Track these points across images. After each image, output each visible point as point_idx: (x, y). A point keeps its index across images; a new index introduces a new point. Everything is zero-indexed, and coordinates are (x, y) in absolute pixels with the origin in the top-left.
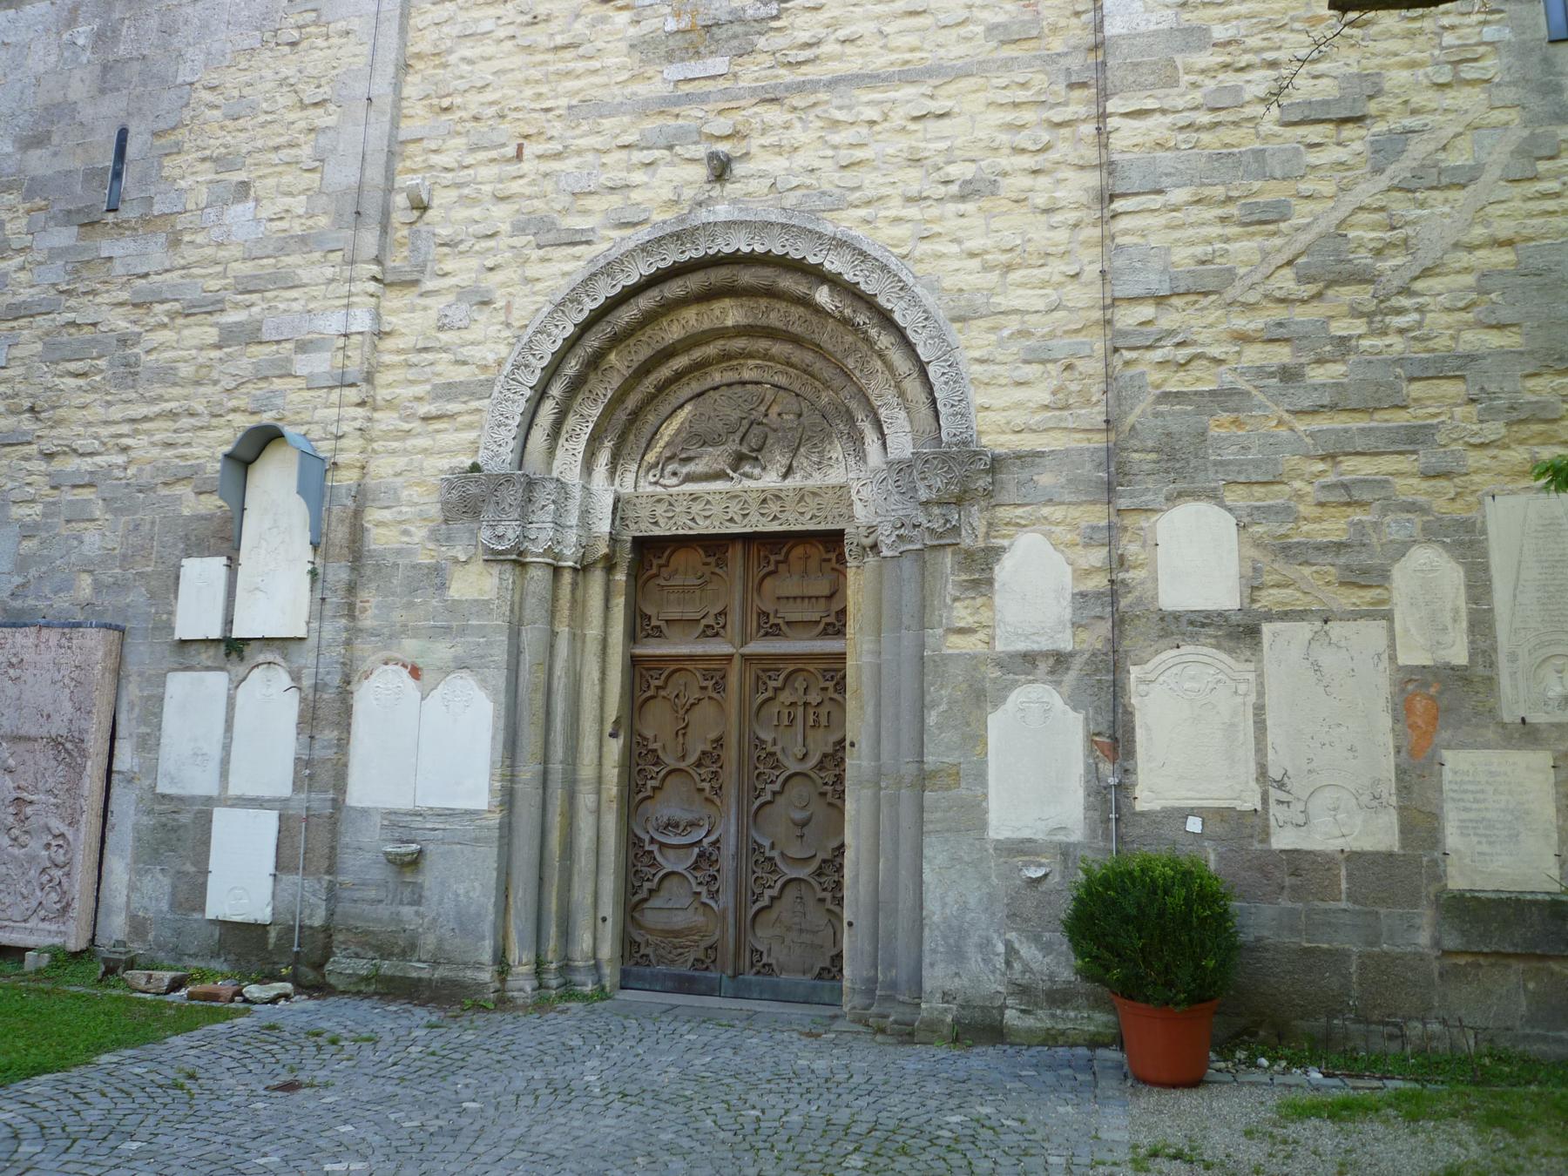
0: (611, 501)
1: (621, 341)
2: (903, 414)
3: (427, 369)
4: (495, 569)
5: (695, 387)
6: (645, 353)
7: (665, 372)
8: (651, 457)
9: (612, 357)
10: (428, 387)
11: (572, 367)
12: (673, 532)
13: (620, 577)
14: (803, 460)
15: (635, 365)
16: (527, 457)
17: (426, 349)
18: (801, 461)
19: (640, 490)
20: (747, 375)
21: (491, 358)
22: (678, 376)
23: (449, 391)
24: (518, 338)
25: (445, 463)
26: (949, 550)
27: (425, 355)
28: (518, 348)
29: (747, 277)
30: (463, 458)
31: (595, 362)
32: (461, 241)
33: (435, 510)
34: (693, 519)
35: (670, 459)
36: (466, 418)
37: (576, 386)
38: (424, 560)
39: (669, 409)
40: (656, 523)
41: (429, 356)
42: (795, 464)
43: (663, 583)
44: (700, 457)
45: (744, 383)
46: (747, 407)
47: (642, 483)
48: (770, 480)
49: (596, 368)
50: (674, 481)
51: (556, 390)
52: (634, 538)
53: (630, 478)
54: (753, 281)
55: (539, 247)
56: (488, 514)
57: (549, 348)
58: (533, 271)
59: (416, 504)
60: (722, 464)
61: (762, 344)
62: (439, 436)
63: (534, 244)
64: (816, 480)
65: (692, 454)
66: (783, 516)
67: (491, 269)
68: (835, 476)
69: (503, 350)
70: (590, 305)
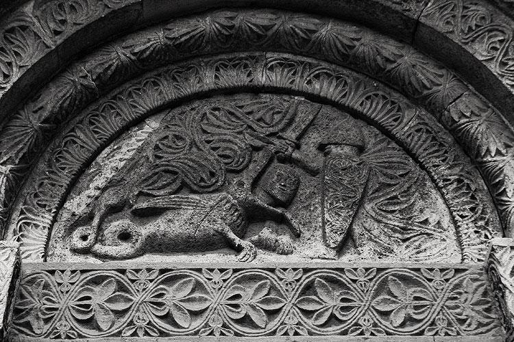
5: (169, 92)
7: (119, 54)
8: (77, 205)
14: (370, 223)
15: (69, 30)
18: (366, 225)
34: (168, 318)
35: (114, 210)
39: (116, 123)
42: (357, 230)
44: (176, 208)
45: (255, 90)
46: (263, 130)
48: (312, 252)
50: (125, 248)
53: (35, 240)
60: (218, 224)
64: (401, 258)
65: (160, 203)
66: (349, 317)
68: (440, 252)
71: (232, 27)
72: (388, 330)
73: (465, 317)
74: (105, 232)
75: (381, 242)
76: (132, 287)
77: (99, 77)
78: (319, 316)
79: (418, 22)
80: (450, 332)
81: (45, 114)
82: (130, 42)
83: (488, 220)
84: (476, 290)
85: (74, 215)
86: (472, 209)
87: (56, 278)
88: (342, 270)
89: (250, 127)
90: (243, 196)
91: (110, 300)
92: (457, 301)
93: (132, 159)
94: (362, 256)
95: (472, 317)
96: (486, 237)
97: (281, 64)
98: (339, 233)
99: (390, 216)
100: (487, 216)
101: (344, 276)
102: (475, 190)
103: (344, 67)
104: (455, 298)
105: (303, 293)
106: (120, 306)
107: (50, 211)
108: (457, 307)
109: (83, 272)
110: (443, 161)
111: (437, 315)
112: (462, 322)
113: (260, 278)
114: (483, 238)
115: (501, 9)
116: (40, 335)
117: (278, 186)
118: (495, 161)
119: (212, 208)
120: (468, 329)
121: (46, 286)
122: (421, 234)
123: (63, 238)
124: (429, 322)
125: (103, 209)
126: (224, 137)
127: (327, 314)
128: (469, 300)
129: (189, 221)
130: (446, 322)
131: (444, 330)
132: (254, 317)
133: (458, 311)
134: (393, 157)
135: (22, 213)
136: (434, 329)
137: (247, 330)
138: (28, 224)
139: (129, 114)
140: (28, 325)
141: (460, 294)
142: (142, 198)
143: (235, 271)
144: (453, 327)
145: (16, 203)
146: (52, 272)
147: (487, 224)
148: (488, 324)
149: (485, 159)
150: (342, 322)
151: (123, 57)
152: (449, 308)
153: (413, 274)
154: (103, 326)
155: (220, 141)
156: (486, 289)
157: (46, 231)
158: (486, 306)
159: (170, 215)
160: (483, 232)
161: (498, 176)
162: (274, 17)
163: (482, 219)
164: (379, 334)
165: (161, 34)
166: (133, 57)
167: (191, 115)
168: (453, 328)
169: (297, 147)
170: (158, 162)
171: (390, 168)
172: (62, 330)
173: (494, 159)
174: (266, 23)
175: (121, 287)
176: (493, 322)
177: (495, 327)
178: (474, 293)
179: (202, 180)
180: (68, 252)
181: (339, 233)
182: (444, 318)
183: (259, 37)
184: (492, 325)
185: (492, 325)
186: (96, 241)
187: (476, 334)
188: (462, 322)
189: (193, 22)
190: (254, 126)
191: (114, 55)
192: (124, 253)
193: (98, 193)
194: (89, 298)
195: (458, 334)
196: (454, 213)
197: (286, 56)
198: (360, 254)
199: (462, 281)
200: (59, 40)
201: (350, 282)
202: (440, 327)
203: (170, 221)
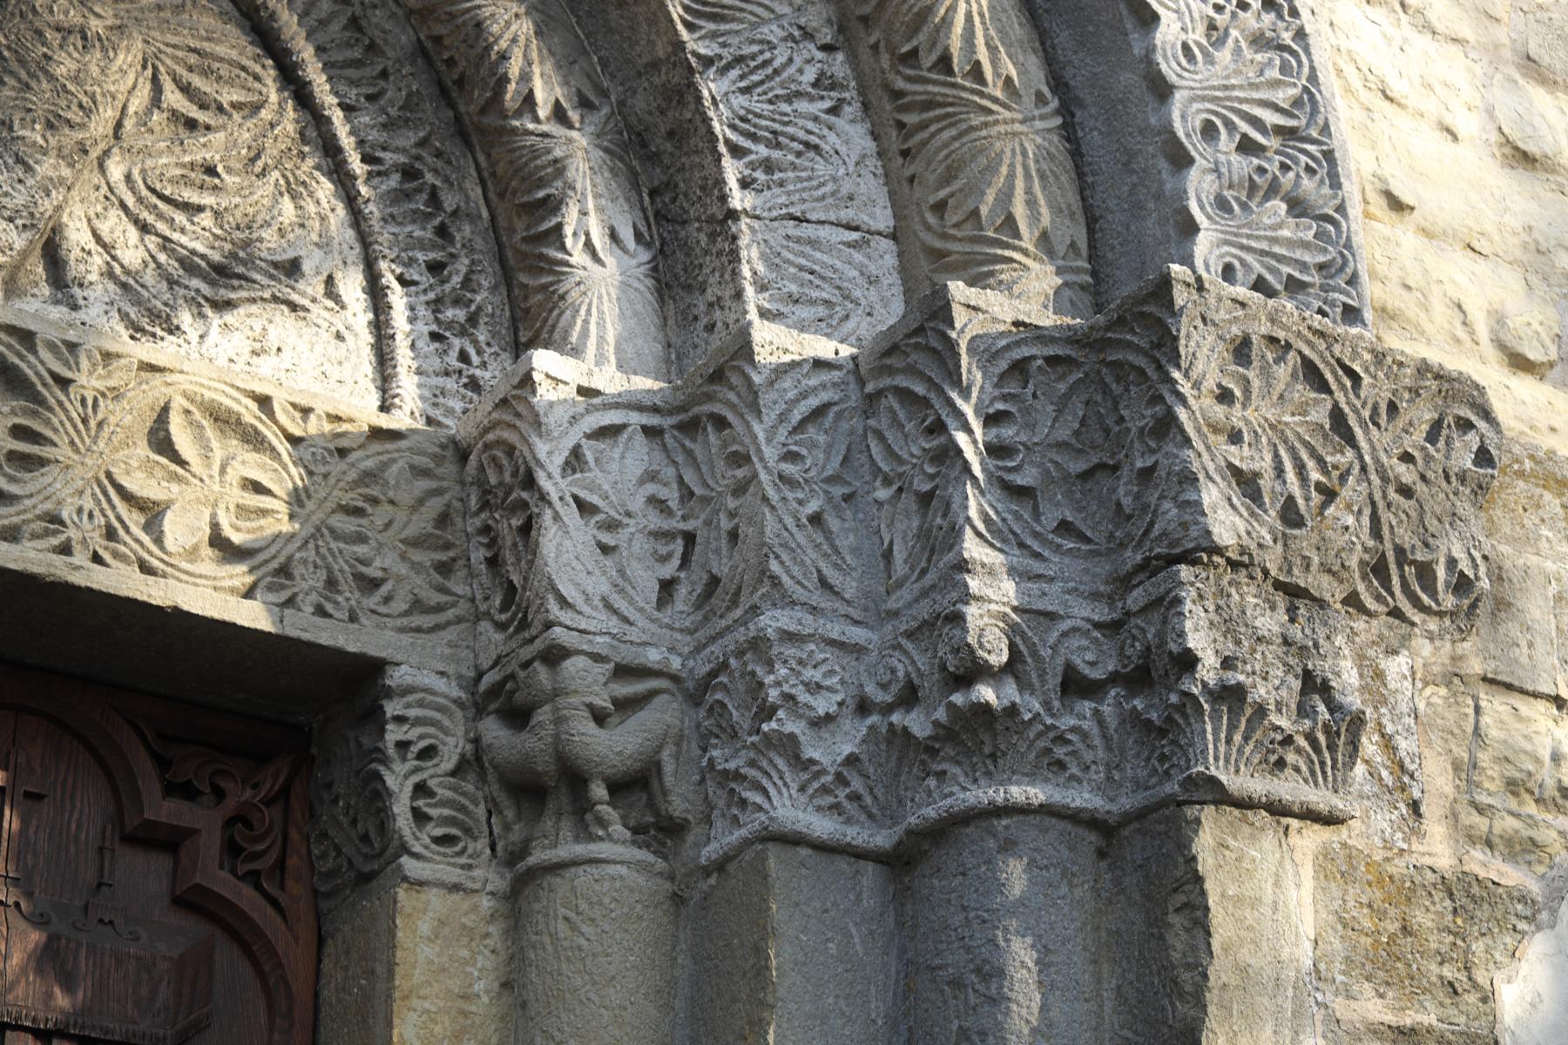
2: (851, 137)
26: (1309, 839)
72: (146, 556)
73: (379, 574)
75: (146, 294)
80: (329, 607)
83: (479, 308)
84: (421, 501)
92: (364, 521)
94: (81, 315)
95: (400, 579)
96: (464, 357)
98: (19, 222)
99: (180, 218)
100: (478, 298)
101: (31, 358)
102: (455, 213)
104: (358, 512)
108: (361, 539)
110: (369, 98)
111: (300, 549)
112: (370, 584)
114: (452, 360)
118: (545, 135)
120: (383, 609)
122: (275, 299)
124: (275, 564)
128: (396, 526)
130: (322, 575)
131: (314, 597)
133: (361, 550)
134: (219, 41)
136: (283, 587)
141: (375, 501)
144: (339, 592)
147: (473, 320)
148: (439, 609)
149: (516, 123)
152: (336, 535)
153: (249, 412)
156: (448, 506)
158: (443, 556)
160: (457, 343)
161: (542, 183)
163: (457, 302)
164: (121, 565)
168: (340, 599)
171: (206, 73)
173: (545, 128)
176: (454, 605)
177: (459, 620)
178: (414, 509)
181: (19, 222)
182: (319, 562)
184: (450, 614)
185: (450, 614)
187: (401, 630)
195: (353, 618)
196: (383, 265)
198: (75, 307)
199: (384, 466)
201: (50, 380)
202: (305, 586)
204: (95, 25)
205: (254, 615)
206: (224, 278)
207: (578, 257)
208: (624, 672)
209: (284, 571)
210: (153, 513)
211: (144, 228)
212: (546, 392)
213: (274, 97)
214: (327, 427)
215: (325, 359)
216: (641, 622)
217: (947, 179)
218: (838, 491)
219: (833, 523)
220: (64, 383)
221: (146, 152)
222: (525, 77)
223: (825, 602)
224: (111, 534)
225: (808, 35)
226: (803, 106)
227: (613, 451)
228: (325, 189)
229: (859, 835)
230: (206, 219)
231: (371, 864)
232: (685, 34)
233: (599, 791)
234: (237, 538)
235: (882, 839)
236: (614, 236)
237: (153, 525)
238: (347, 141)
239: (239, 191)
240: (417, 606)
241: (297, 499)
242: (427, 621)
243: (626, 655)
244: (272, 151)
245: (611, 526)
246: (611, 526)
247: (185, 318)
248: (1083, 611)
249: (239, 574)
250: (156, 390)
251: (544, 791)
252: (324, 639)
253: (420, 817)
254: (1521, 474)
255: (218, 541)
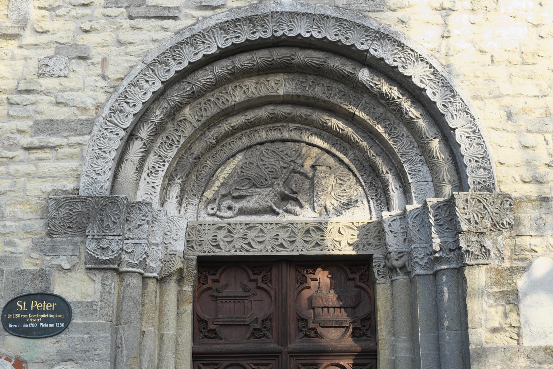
0: (185, 226)
1: (196, 99)
2: (425, 168)
3: (29, 108)
4: (98, 276)
5: (246, 141)
6: (213, 110)
7: (225, 127)
8: (209, 194)
9: (187, 111)
10: (31, 123)
11: (158, 115)
12: (233, 253)
13: (188, 288)
15: (204, 119)
16: (118, 186)
17: (28, 92)
19: (201, 219)
20: (287, 135)
21: (90, 102)
22: (235, 131)
23: (50, 126)
24: (115, 88)
25: (48, 186)
26: (484, 268)
27: (26, 96)
28: (115, 96)
29: (303, 56)
30: (65, 183)
31: (173, 113)
32: (59, 7)
33: (38, 225)
34: (249, 244)
36: (67, 150)
37: (158, 130)
38: (27, 265)
39: (224, 156)
40: (218, 246)
41: (31, 97)
43: (217, 295)
44: (251, 195)
45: (284, 141)
46: (288, 160)
47: (203, 214)
49: (173, 119)
50: (229, 213)
51: (144, 133)
52: (199, 257)
53: (192, 210)
54: (307, 60)
55: (131, 17)
56: (93, 229)
57: (141, 98)
58: (127, 36)
59: (20, 220)
60: (269, 202)
61: (304, 112)
62: (41, 164)
63: (125, 15)
65: (244, 193)
67: (87, 31)
69: (102, 98)
70: (175, 67)
71: (274, 114)
74: (221, 206)
76: (234, 231)
77: (216, 138)
78: (311, 243)
79: (354, 114)
81: (194, 156)
82: (229, 121)
85: (208, 199)
86: (376, 195)
87: (203, 227)
88: (321, 223)
89: (282, 158)
90: (279, 190)
91: (225, 237)
93: (231, 173)
97: (295, 129)
99: (341, 198)
103: (323, 130)
105: (305, 233)
106: (229, 239)
107: (198, 197)
108: (367, 238)
109: (213, 224)
112: (369, 244)
113: (287, 227)
115: (389, 110)
116: (197, 251)
117: (294, 185)
119: (266, 195)
121: (199, 231)
123: (204, 209)
125: (220, 196)
126: (271, 163)
127: (315, 242)
129: (257, 202)
132: (285, 244)
133: (368, 240)
135: (187, 199)
137: (282, 249)
138: (189, 203)
139: (229, 152)
140: (192, 247)
142: (236, 190)
143: (277, 224)
145: (184, 194)
146: (201, 225)
147: (381, 202)
150: (320, 245)
151: (226, 129)
153: (351, 225)
154: (222, 248)
155: (269, 164)
157: (197, 207)
159: (248, 199)
161: (386, 183)
162: (292, 109)
163: (379, 200)
165: (243, 118)
166: (231, 129)
167: (256, 152)
169: (303, 166)
170: (242, 174)
171: (343, 176)
172: (206, 250)
174: (288, 111)
175: (229, 231)
179: (262, 182)
180: (206, 215)
183: (286, 117)
186: (218, 210)
188: (369, 244)
189: (257, 111)
190: (284, 157)
191: (222, 128)
192: (229, 216)
193: (217, 189)
194: (216, 236)
197: (297, 125)
200: (200, 124)
203: (248, 201)
204: (327, 175)
205: (354, 253)
206: (348, 205)
207: (391, 192)
208: (399, 253)
209: (358, 245)
210: (340, 243)
211: (337, 200)
212: (384, 217)
213: (352, 177)
214: (362, 224)
215: (363, 214)
216: (401, 246)
217: (436, 174)
218: (422, 225)
219: (421, 230)
220: (326, 228)
221: (336, 190)
222: (382, 168)
223: (421, 242)
224: (334, 247)
225: (418, 154)
226: (418, 165)
227: (395, 222)
228: (360, 188)
229: (428, 272)
230: (345, 197)
231: (374, 282)
232: (401, 158)
233: (398, 270)
234: (351, 243)
235: (432, 273)
236: (396, 188)
237: (340, 244)
238: (362, 181)
239: (349, 192)
240: (376, 246)
241: (358, 235)
242: (377, 247)
243: (399, 251)
244: (353, 185)
245: (396, 233)
246: (396, 233)
247: (343, 212)
248: (451, 240)
249: (351, 248)
250: (338, 225)
251: (393, 269)
252: (364, 254)
253: (379, 275)
254: (524, 201)
255: (348, 244)
